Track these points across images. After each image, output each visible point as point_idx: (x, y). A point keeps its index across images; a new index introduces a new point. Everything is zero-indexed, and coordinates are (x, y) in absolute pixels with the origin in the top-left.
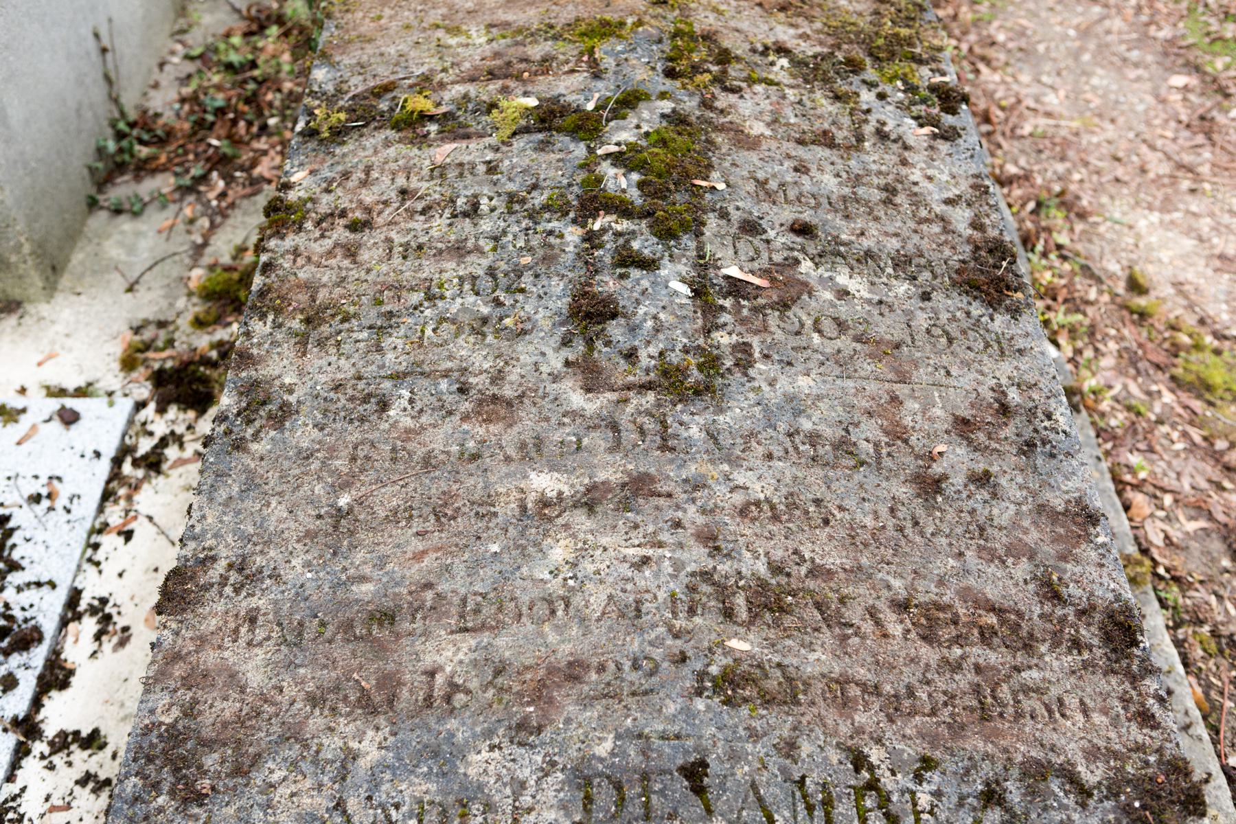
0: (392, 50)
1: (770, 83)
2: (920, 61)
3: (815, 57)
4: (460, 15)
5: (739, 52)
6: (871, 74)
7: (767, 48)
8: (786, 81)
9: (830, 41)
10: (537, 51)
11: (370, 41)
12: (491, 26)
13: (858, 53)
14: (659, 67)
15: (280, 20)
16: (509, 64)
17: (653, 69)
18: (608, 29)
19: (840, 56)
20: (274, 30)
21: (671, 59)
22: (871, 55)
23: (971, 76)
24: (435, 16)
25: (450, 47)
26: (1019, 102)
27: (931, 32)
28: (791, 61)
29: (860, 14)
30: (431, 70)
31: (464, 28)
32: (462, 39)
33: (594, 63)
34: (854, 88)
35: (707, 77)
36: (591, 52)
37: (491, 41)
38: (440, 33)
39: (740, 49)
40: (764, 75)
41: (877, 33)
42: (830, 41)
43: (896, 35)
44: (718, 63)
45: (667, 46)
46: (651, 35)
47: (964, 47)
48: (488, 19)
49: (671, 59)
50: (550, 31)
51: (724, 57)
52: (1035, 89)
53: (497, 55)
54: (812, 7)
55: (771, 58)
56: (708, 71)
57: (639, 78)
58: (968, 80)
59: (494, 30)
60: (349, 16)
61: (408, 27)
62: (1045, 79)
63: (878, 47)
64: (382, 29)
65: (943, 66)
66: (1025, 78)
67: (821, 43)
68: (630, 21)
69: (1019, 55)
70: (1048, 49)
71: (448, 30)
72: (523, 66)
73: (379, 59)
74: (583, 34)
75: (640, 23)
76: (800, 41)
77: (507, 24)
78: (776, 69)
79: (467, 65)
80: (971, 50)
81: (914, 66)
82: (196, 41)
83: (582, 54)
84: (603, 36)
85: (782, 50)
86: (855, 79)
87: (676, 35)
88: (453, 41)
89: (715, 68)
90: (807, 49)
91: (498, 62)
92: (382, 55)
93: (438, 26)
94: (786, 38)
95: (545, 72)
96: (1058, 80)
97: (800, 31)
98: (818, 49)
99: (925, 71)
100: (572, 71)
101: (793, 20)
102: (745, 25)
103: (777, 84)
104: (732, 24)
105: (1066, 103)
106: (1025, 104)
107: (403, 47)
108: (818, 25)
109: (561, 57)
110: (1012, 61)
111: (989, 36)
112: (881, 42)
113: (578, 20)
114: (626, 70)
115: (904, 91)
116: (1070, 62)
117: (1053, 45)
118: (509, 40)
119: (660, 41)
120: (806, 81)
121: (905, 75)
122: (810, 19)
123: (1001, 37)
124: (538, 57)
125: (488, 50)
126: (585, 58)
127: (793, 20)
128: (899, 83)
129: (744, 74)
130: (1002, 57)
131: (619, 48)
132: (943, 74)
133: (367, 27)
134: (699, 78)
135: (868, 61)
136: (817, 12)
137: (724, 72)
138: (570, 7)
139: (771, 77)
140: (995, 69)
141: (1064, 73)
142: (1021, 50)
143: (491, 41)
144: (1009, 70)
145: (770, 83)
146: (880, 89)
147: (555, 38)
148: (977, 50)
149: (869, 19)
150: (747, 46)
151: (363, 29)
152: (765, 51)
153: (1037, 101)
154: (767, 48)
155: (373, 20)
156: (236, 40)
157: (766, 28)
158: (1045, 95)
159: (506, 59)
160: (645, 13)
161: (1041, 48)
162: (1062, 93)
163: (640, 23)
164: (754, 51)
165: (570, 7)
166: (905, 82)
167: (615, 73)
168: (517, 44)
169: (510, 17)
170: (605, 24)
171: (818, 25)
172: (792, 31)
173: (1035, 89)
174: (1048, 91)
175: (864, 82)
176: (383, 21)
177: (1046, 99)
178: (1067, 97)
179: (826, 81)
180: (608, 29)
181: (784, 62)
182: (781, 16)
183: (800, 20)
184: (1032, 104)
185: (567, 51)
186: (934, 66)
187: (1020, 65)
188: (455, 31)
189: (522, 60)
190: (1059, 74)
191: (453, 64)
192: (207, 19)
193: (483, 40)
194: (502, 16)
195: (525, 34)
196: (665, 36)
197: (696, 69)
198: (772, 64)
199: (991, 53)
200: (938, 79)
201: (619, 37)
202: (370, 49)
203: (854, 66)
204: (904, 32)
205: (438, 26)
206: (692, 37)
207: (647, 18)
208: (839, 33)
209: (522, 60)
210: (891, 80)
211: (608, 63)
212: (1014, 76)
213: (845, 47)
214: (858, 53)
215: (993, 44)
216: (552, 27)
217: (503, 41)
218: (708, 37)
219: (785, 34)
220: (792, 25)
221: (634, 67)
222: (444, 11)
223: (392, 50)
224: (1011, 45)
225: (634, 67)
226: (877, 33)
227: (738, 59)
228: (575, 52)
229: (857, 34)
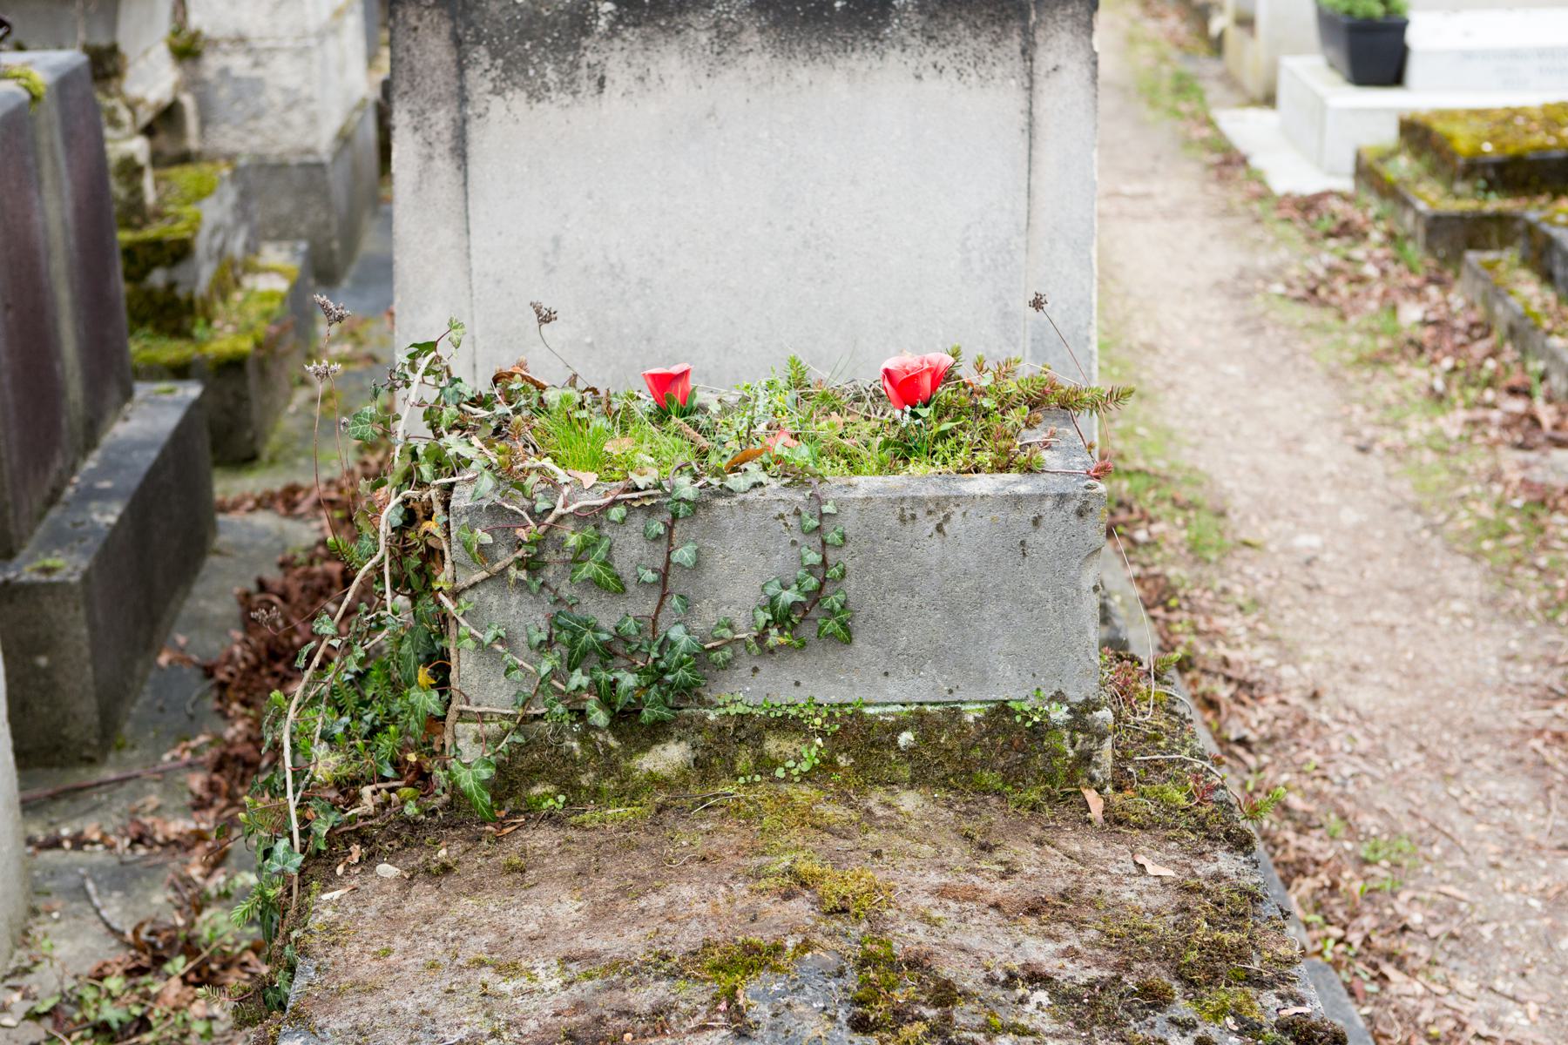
0: (409, 1005)
1: (1022, 1031)
2: (1261, 984)
3: (1091, 986)
4: (517, 944)
5: (969, 984)
6: (1182, 1008)
7: (1012, 976)
8: (1046, 1028)
9: (1113, 958)
10: (643, 998)
11: (373, 990)
12: (569, 959)
13: (1160, 975)
14: (842, 1015)
15: (190, 948)
16: (599, 1020)
17: (833, 1018)
18: (756, 958)
19: (1131, 982)
20: (179, 965)
21: (860, 1002)
22: (1180, 977)
23: (1373, 988)
24: (476, 947)
25: (502, 996)
26: (1462, 1026)
27: (1272, 935)
28: (1052, 994)
29: (1157, 913)
30: (473, 1035)
31: (525, 964)
32: (522, 982)
33: (737, 1015)
34: (1157, 1033)
35: (920, 1028)
36: (732, 995)
37: (568, 984)
38: (486, 975)
39: (969, 978)
40: (1012, 1019)
41: (1186, 942)
42: (1113, 958)
43: (1217, 943)
44: (938, 1003)
45: (852, 981)
46: (826, 965)
47: (1356, 938)
48: (563, 948)
49: (860, 1002)
50: (663, 965)
51: (946, 995)
52: (1485, 1003)
53: (579, 1006)
54: (1079, 905)
55: (1020, 992)
56: (921, 1018)
57: (810, 1034)
58: (1367, 995)
59: (573, 967)
60: (338, 951)
61: (433, 966)
62: (1499, 985)
63: (1191, 965)
64: (391, 969)
65: (1297, 989)
66: (1466, 985)
67: (1098, 963)
68: (790, 943)
69: (1451, 945)
70: (1498, 931)
71: (499, 969)
72: (623, 1022)
73: (388, 1020)
74: (718, 968)
75: (806, 946)
76: (1065, 961)
77: (595, 955)
78: (1030, 1008)
79: (532, 1025)
80: (1367, 941)
81: (1252, 991)
82: (47, 985)
83: (716, 999)
84: (750, 969)
85: (1036, 978)
86: (1159, 1018)
87: (865, 962)
88: (507, 987)
89: (931, 1013)
90: (1079, 974)
91: (581, 1018)
92: (393, 1012)
93: (482, 964)
94: (1041, 957)
95: (661, 1031)
96: (1522, 984)
97: (1064, 945)
98: (1095, 973)
99: (1269, 998)
100: (703, 1028)
101: (1051, 929)
102: (974, 941)
103: (1034, 1033)
104: (954, 939)
105: (1542, 1023)
106: (1471, 1030)
107: (427, 1000)
108: (1091, 934)
109: (683, 1006)
110: (1441, 958)
111: (1396, 917)
112: (1193, 956)
113: (707, 945)
114: (789, 1022)
115: (1240, 1034)
116: (1539, 953)
117: (1505, 925)
118: (597, 982)
119: (841, 973)
120: (1080, 1026)
121: (1238, 1007)
122: (1079, 925)
123: (1416, 919)
124: (646, 1008)
125: (564, 999)
126: (723, 1006)
127: (1051, 929)
128: (1230, 1021)
129: (980, 1020)
130: (1423, 951)
131: (775, 987)
132: (1300, 1002)
133: (367, 969)
134: (907, 1031)
135: (1177, 987)
136: (1087, 914)
137: (947, 1018)
138: (694, 925)
139: (1023, 1021)
140: (1413, 974)
141: (1531, 972)
142: (1452, 936)
143: (568, 984)
144: (1438, 973)
145: (1022, 1031)
146: (1199, 1032)
147: (671, 975)
148: (1378, 941)
149: (1172, 919)
150: (980, 974)
151: (360, 972)
152: (1011, 981)
153: (1492, 1025)
154: (1012, 976)
155: (377, 957)
156: (114, 983)
157: (1009, 943)
158: (1505, 1012)
159: (596, 1012)
160: (814, 929)
161: (1487, 931)
162: (1533, 1008)
163: (806, 946)
164: (992, 981)
165: (694, 925)
166: (1239, 1019)
167: (772, 1028)
168: (611, 987)
169: (598, 944)
170: (751, 949)
171: (1091, 934)
172: (1051, 946)
173: (1485, 1003)
174: (1511, 1004)
175: (1173, 1021)
176: (392, 958)
177: (1509, 1020)
178: (1541, 1012)
179: (1112, 1023)
180: (756, 958)
181: (1042, 996)
182: (1031, 922)
183: (1062, 928)
184: (1485, 1031)
185: (693, 995)
186: (1283, 990)
187: (1454, 962)
188: (509, 969)
189: (620, 1014)
190: (1524, 975)
191: (509, 1023)
192: (64, 949)
193: (555, 983)
194: (584, 943)
195: (624, 970)
196: (849, 965)
197: (902, 1015)
198: (1023, 1001)
199: (1403, 945)
200: (1292, 1010)
201: (775, 969)
202: (372, 1004)
203: (1155, 998)
204: (1229, 937)
205: (482, 964)
206: (892, 964)
207: (818, 938)
208: (1126, 943)
209: (620, 1014)
210: (1217, 1016)
211: (760, 1012)
212: (1446, 983)
213: (1138, 966)
214: (1160, 975)
215: (1405, 929)
216: (666, 958)
217: (588, 984)
218: (916, 963)
219: (1039, 951)
220: (1050, 936)
221: (801, 1018)
222: (491, 937)
223: (409, 1005)
224: (1434, 930)
225: (801, 1018)
226: (1186, 942)
227: (967, 996)
228: (706, 998)
229: (1155, 945)
